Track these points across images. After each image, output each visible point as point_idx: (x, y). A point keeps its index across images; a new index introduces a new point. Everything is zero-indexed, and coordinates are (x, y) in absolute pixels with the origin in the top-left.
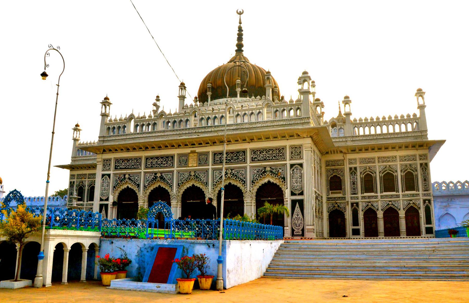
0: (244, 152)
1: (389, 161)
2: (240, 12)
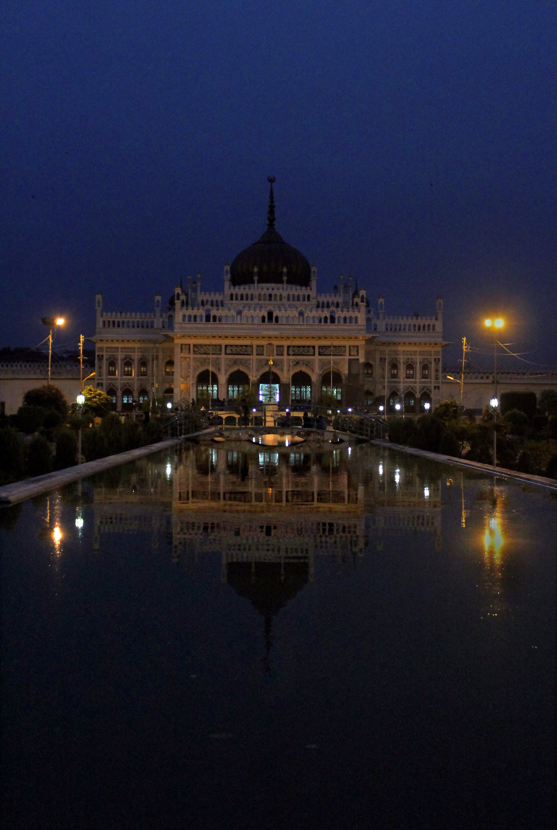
0: (314, 347)
1: (411, 355)
2: (271, 179)
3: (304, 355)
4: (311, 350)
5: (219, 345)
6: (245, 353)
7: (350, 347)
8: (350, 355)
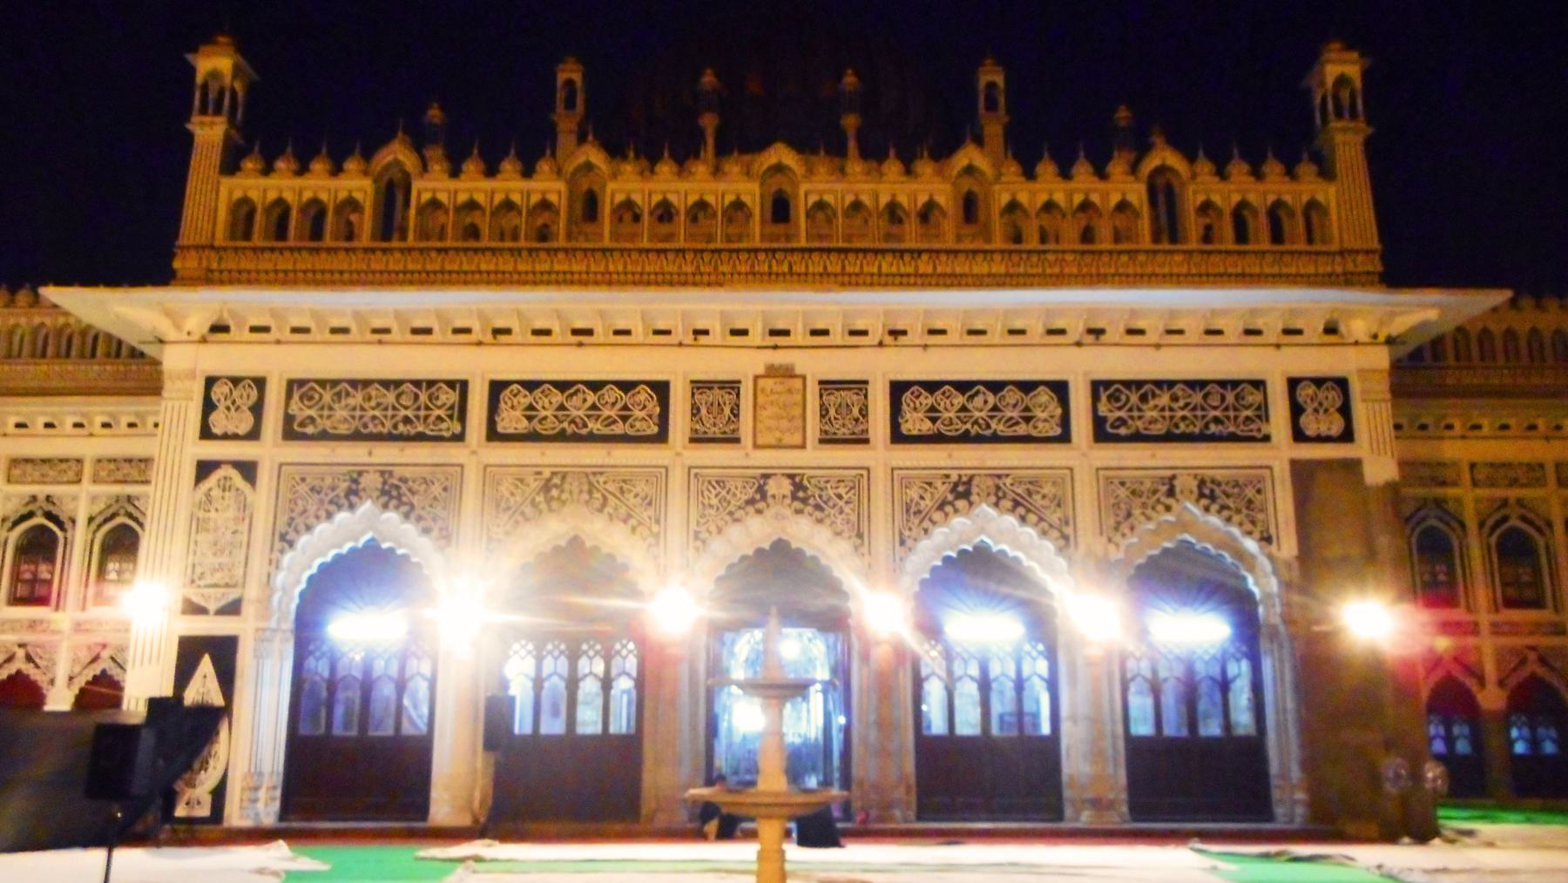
0: (1060, 389)
1: (1514, 482)
3: (996, 439)
4: (1045, 406)
5: (451, 384)
6: (619, 429)
7: (1293, 383)
8: (1299, 436)
